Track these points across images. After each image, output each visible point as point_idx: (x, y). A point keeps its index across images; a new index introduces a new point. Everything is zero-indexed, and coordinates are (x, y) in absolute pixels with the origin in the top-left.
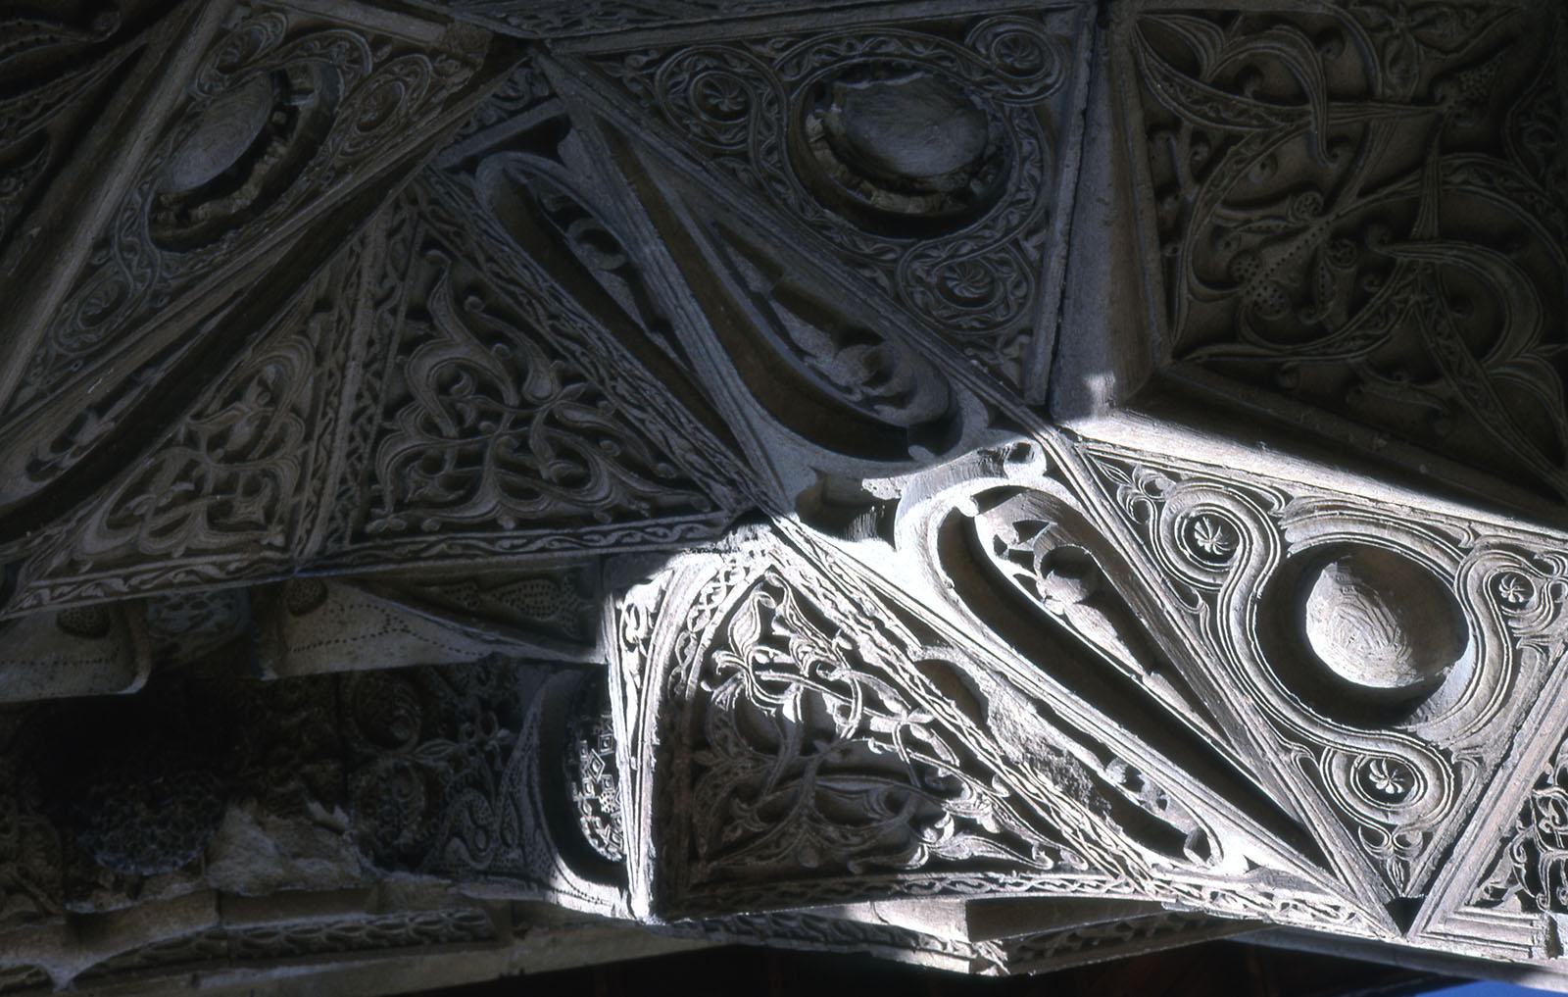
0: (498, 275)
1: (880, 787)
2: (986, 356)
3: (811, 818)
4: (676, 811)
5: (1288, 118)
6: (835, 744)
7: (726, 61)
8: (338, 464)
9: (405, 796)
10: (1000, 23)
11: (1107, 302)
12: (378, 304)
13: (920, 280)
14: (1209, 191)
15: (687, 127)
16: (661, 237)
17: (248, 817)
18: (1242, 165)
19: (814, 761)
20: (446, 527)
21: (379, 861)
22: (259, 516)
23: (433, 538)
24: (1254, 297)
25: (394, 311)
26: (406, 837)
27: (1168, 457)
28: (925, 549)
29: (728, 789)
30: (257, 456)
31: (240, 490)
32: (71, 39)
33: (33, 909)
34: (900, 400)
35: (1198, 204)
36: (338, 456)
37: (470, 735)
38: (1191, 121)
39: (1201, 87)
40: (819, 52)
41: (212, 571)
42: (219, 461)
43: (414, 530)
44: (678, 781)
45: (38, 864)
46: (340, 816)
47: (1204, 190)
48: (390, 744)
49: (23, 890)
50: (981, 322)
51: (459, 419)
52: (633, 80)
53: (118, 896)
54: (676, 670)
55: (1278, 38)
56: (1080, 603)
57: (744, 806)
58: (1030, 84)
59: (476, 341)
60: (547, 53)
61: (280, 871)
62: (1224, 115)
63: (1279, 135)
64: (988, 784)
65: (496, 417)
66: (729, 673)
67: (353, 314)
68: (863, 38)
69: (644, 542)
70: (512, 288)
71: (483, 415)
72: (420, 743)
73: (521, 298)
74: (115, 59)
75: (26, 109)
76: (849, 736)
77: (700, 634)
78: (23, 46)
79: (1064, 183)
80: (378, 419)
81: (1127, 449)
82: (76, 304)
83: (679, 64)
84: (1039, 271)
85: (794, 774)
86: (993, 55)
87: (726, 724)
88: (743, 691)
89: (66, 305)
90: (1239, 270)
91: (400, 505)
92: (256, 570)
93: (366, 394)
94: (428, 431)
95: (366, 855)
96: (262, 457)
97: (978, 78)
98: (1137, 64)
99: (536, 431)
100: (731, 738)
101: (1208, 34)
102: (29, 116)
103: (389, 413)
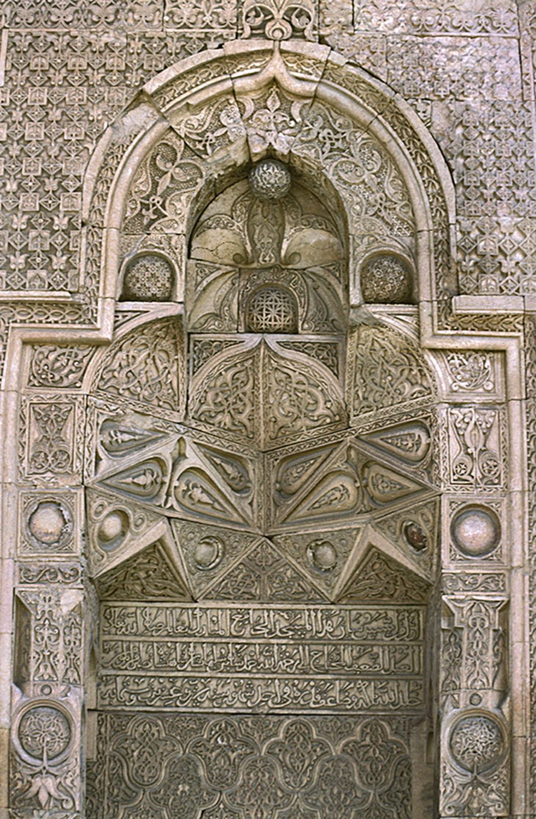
8: (260, 375)
20: (235, 365)
36: (261, 381)
71: (236, 403)
84: (182, 547)
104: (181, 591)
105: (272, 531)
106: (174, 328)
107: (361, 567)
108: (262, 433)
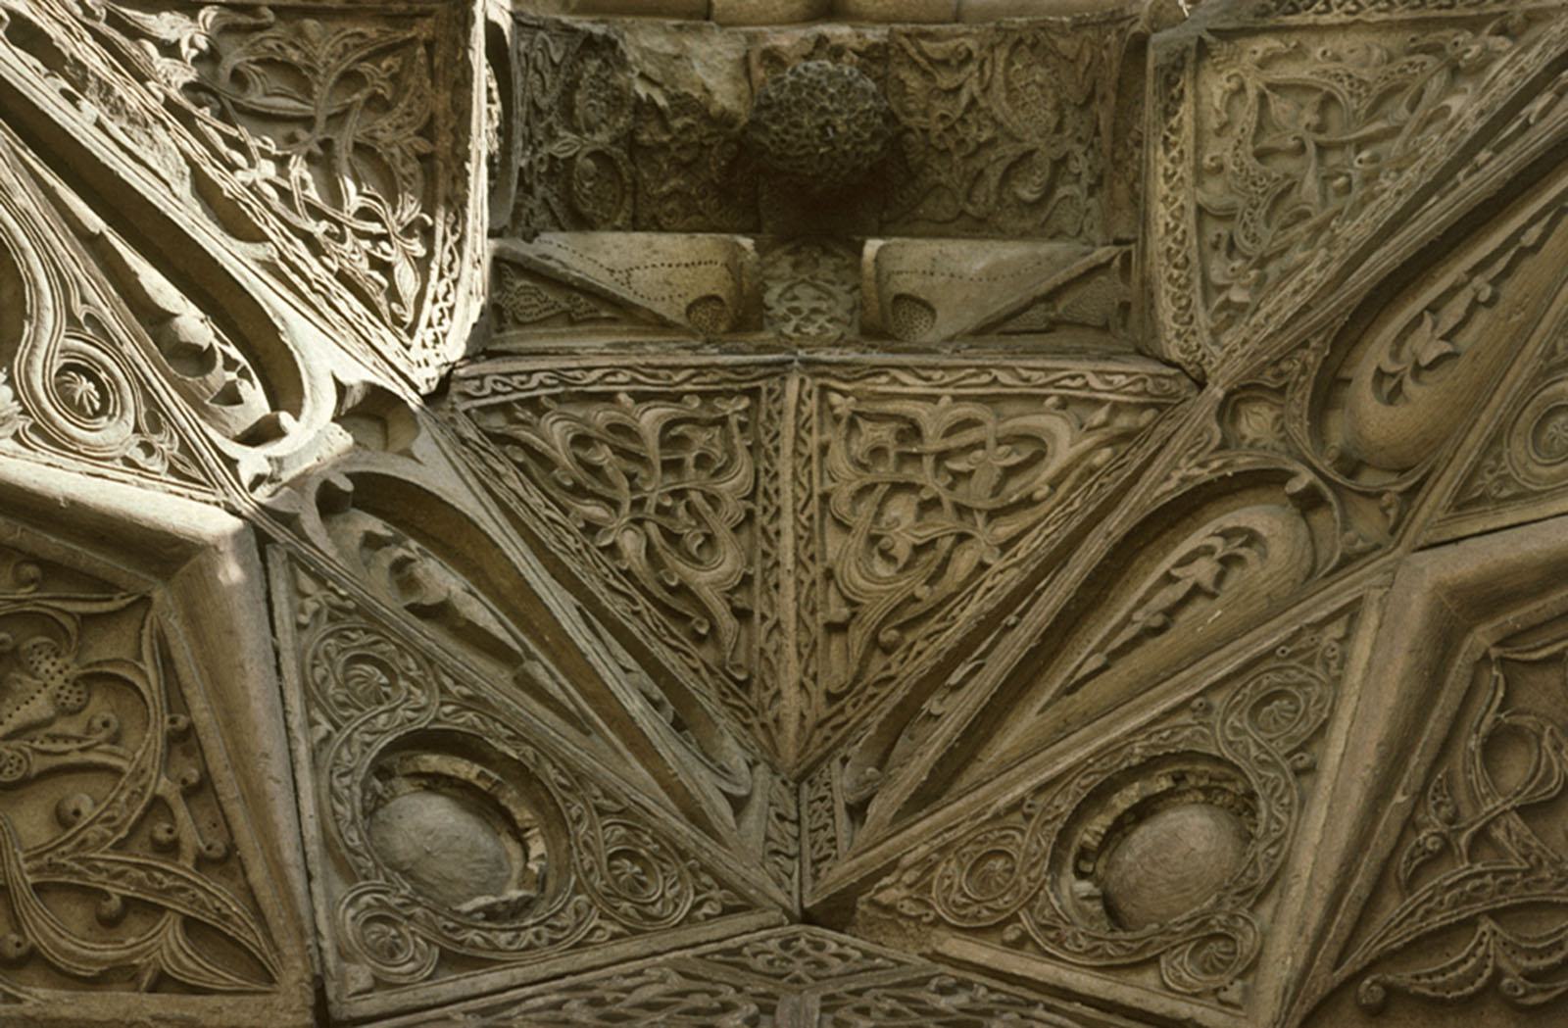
0: (688, 655)
1: (255, 98)
2: (335, 600)
3: (315, 72)
4: (448, 94)
5: (54, 867)
6: (304, 150)
7: (638, 911)
8: (785, 466)
9: (591, 105)
10: (413, 973)
11: (248, 667)
12: (777, 624)
13: (414, 682)
14: (144, 787)
15: (655, 841)
16: (632, 719)
17: (717, 97)
18: (106, 815)
19: (320, 132)
20: (677, 398)
21: (613, 45)
22: (865, 426)
23: (688, 387)
24: (59, 662)
25: (764, 618)
26: (593, 65)
27: (140, 485)
28: (310, 376)
29: (397, 112)
30: (880, 487)
31: (892, 454)
32: (1401, 976)
33: (925, 44)
34: (371, 541)
35: (155, 774)
36: (786, 476)
37: (541, 161)
38: (184, 868)
39: (179, 905)
40: (563, 929)
41: (904, 377)
42: (922, 487)
43: (706, 396)
44: (446, 124)
45: (914, 82)
46: (641, 89)
47: (150, 789)
48: (595, 155)
49: (931, 61)
50: (347, 638)
51: (689, 507)
52: (710, 888)
53: (840, 41)
54: (456, 238)
55: (88, 961)
56: (176, 315)
57: (380, 91)
58: (369, 906)
59: (692, 588)
60: (786, 911)
61: (687, 43)
62: (142, 874)
63: (65, 848)
64: (167, 97)
65: (661, 510)
66: (408, 231)
67: (798, 615)
68: (530, 947)
69: (509, 375)
70: (674, 643)
72: (576, 155)
73: (664, 632)
74: (1357, 959)
75: (1428, 912)
76: (294, 158)
77: (441, 276)
78: (1443, 972)
79: (310, 797)
80: (759, 511)
81: (178, 494)
82: (1313, 717)
83: (676, 906)
84: (309, 698)
85: (338, 118)
86: (409, 936)
87: (404, 178)
88: (394, 212)
89: (1325, 716)
90: (79, 693)
91: (723, 421)
92: (856, 372)
93: (773, 536)
94: (713, 497)
95: (622, 52)
96: (874, 486)
97: (418, 910)
98: (268, 935)
99: (626, 499)
100: (398, 163)
101: (178, 962)
102: (1426, 906)
103: (750, 515)
104: (251, 937)
105: (840, 873)
106: (433, 73)
107: (1417, 762)
108: (791, 693)
